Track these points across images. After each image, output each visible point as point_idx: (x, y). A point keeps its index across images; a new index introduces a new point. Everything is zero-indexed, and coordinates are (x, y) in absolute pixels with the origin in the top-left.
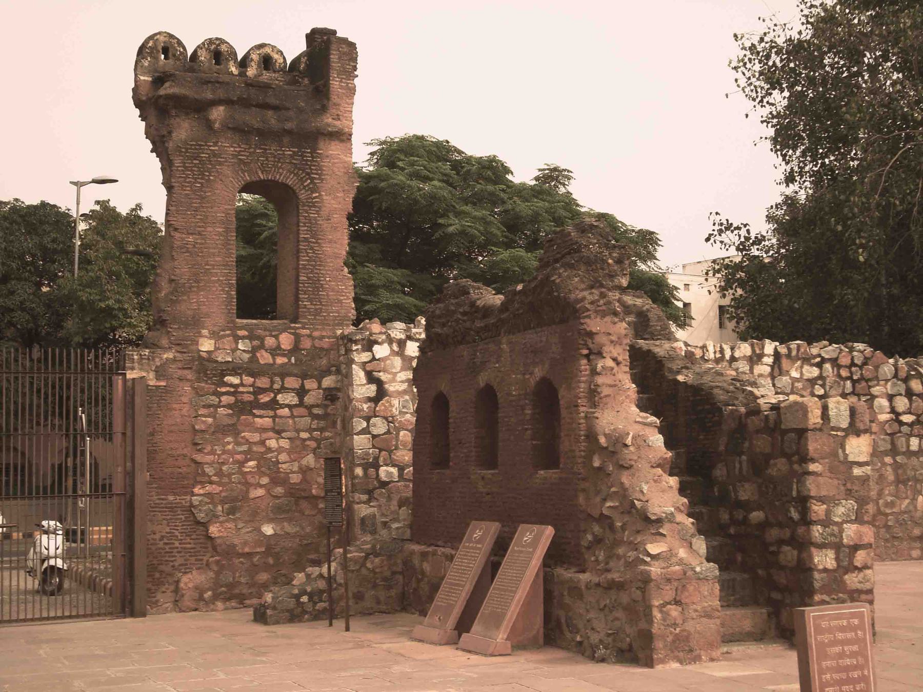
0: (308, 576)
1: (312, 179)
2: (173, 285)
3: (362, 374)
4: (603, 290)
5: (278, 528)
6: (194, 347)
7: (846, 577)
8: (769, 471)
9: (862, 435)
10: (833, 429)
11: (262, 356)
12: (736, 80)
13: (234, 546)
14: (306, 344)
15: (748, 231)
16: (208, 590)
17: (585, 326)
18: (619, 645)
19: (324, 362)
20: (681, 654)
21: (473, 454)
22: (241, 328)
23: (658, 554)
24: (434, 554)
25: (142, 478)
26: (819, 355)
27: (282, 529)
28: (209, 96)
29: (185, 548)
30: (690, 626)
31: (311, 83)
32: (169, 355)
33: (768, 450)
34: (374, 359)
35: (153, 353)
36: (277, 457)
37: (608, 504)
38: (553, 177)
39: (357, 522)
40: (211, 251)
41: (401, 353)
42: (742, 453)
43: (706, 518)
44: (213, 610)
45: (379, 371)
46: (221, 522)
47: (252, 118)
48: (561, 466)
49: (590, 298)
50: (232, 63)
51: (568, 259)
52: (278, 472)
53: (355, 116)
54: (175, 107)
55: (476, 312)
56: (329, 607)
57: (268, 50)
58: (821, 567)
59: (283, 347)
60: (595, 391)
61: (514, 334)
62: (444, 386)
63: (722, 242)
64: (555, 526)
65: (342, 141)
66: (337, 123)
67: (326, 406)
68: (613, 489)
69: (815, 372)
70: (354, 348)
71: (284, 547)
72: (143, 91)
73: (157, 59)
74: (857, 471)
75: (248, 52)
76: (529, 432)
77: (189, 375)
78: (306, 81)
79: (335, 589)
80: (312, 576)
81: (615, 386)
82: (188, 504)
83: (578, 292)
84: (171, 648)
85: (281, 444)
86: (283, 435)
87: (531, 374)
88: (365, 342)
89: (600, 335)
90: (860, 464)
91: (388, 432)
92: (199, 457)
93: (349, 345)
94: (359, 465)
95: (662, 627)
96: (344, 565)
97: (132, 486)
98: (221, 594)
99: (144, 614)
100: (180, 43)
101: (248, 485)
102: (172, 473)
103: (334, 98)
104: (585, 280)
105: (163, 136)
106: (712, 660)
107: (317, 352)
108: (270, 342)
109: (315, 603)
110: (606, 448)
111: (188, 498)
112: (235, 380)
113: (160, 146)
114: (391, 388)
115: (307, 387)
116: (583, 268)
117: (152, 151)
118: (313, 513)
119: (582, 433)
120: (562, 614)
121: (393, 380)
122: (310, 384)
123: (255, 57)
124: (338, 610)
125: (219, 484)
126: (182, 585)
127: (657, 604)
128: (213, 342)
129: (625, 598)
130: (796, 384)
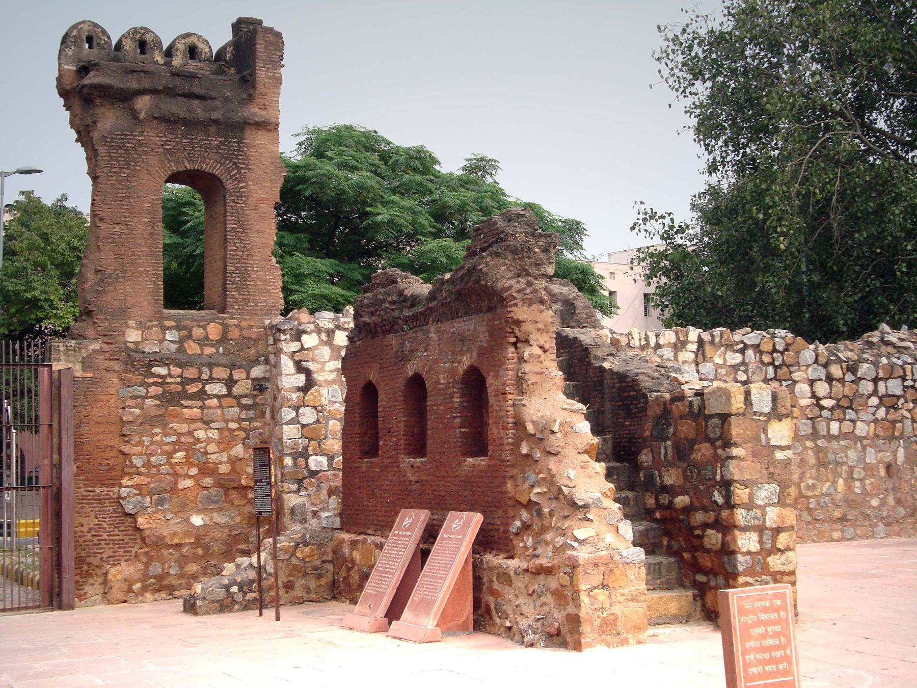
0: (238, 566)
1: (239, 169)
2: (99, 275)
3: (291, 364)
4: (530, 278)
5: (207, 519)
6: (120, 338)
7: (769, 559)
8: (694, 456)
9: (784, 419)
10: (755, 413)
11: (190, 346)
12: (660, 71)
13: (162, 538)
14: (235, 334)
15: (672, 220)
16: (137, 581)
17: (512, 315)
18: (548, 630)
19: (253, 351)
20: (609, 638)
21: (402, 442)
22: (169, 318)
23: (585, 540)
24: (364, 542)
25: (69, 470)
26: (742, 342)
27: (212, 519)
28: (134, 85)
29: (113, 540)
30: (617, 610)
31: (238, 72)
32: (96, 346)
33: (692, 435)
34: (302, 349)
35: (80, 344)
36: (205, 448)
37: (536, 490)
38: (480, 167)
39: (287, 511)
41: (329, 343)
42: (668, 438)
43: (632, 503)
44: (142, 602)
45: (308, 361)
46: (150, 514)
47: (177, 107)
48: (489, 453)
49: (517, 286)
50: (157, 52)
51: (495, 248)
52: (207, 462)
53: (282, 105)
54: (100, 97)
55: (404, 301)
56: (261, 597)
57: (193, 39)
58: (744, 550)
59: (211, 337)
60: (522, 378)
61: (442, 322)
62: (373, 376)
63: (646, 231)
64: (483, 512)
65: (270, 130)
66: (264, 113)
67: (255, 396)
68: (541, 476)
69: (738, 358)
70: (283, 338)
71: (213, 538)
72: (68, 83)
73: (81, 47)
74: (779, 455)
75: (174, 41)
76: (458, 420)
77: (116, 366)
78: (232, 71)
79: (265, 579)
80: (242, 567)
81: (542, 373)
82: (116, 496)
83: (504, 281)
84: (100, 640)
85: (212, 434)
86: (211, 425)
87: (459, 362)
88: (293, 332)
89: (527, 323)
90: (782, 448)
91: (318, 421)
92: (126, 449)
93: (278, 334)
94: (289, 455)
95: (590, 611)
96: (274, 556)
97: (59, 478)
98: (150, 585)
99: (71, 607)
100: (104, 32)
101: (176, 475)
102: (100, 465)
103: (260, 88)
104: (512, 268)
105: (88, 126)
106: (639, 642)
107: (246, 342)
108: (198, 332)
109: (245, 594)
110: (534, 435)
111: (116, 489)
112: (163, 371)
113: (84, 136)
114: (318, 377)
115: (235, 378)
116: (510, 256)
117: (77, 141)
118: (243, 503)
119: (510, 420)
120: (491, 600)
121: (322, 370)
122: (238, 375)
123: (180, 46)
124: (267, 598)
125: (147, 475)
126: (110, 577)
127: (584, 588)
128: (140, 332)
129: (553, 583)
130: (720, 371)
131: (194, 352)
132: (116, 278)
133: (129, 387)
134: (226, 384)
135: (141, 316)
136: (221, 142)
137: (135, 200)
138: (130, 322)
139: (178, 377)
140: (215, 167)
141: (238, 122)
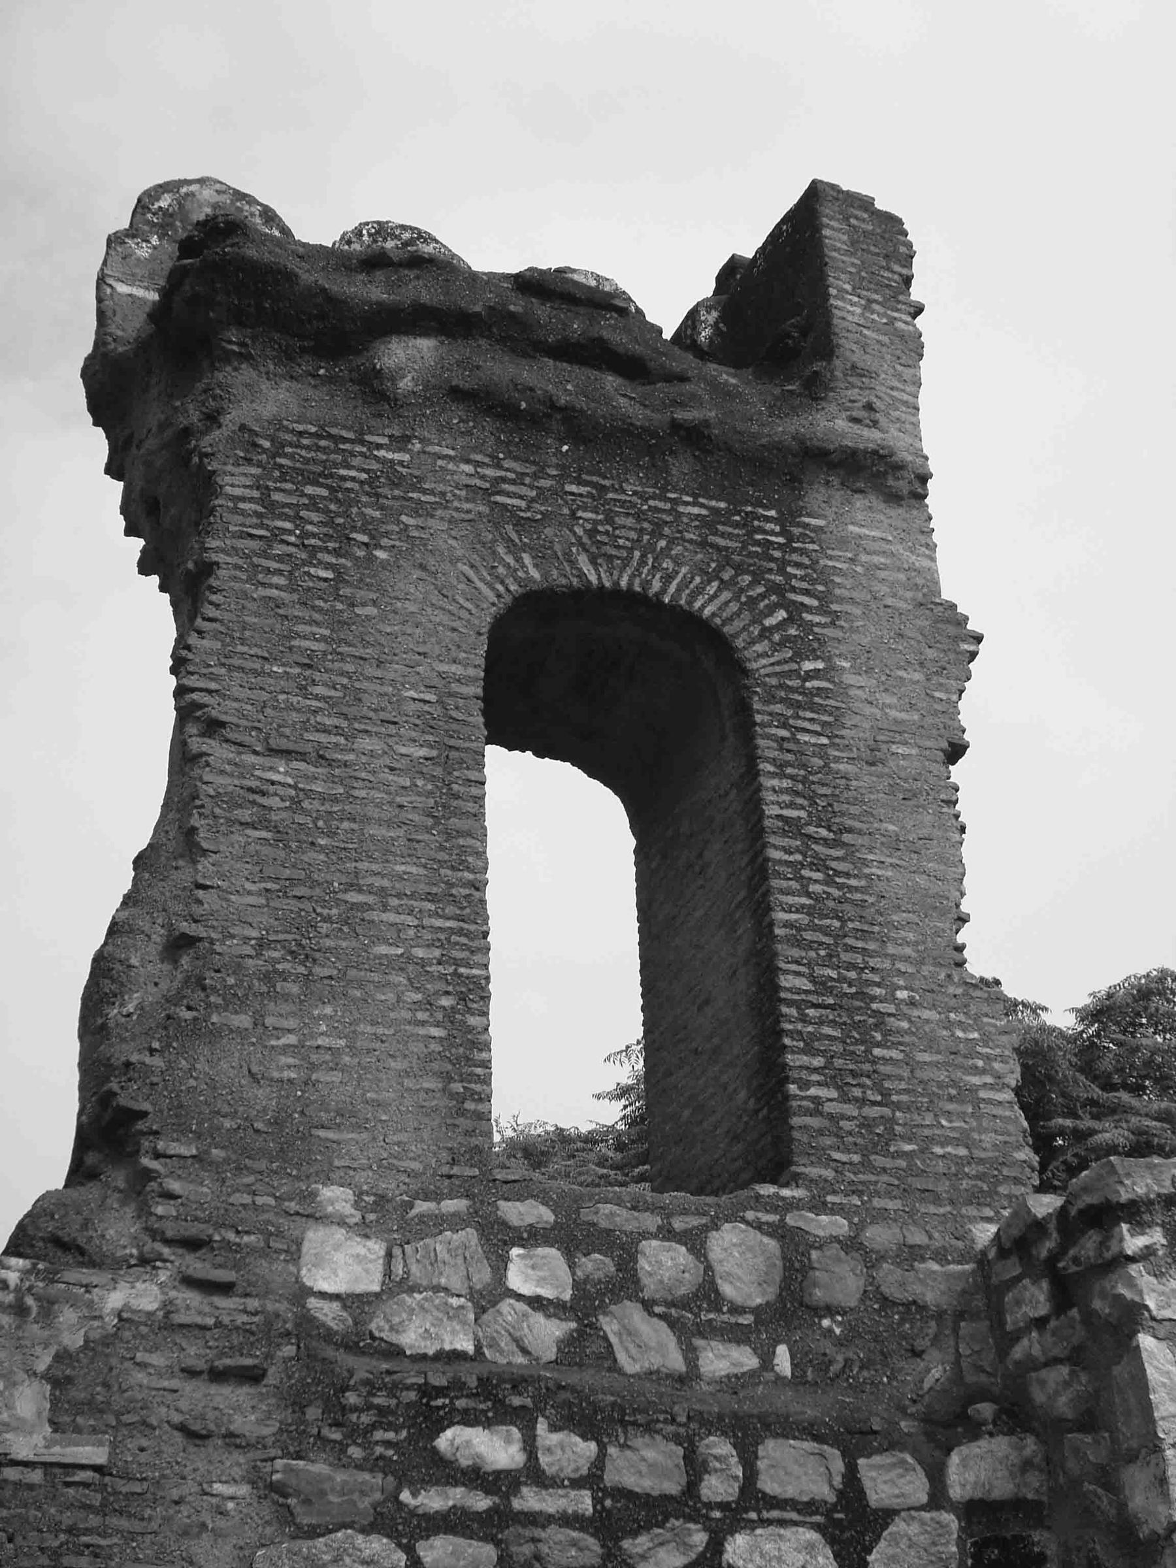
2: (185, 961)
6: (272, 1270)
11: (629, 1332)
14: (840, 1282)
19: (936, 1373)
32: (141, 1295)
35: (51, 1278)
40: (373, 830)
59: (727, 1289)
65: (893, 498)
77: (244, 1410)
93: (1088, 1246)
100: (269, 216)
103: (849, 349)
108: (664, 1264)
112: (496, 1448)
128: (377, 1248)
131: (654, 1361)
132: (267, 977)
133: (313, 1533)
134: (832, 1533)
135: (384, 1167)
136: (715, 511)
137: (371, 671)
138: (328, 1193)
139: (577, 1483)
140: (699, 590)
141: (778, 447)
